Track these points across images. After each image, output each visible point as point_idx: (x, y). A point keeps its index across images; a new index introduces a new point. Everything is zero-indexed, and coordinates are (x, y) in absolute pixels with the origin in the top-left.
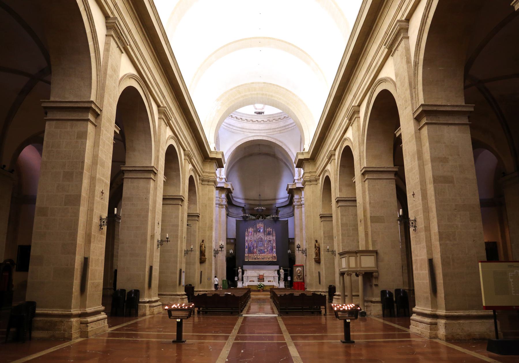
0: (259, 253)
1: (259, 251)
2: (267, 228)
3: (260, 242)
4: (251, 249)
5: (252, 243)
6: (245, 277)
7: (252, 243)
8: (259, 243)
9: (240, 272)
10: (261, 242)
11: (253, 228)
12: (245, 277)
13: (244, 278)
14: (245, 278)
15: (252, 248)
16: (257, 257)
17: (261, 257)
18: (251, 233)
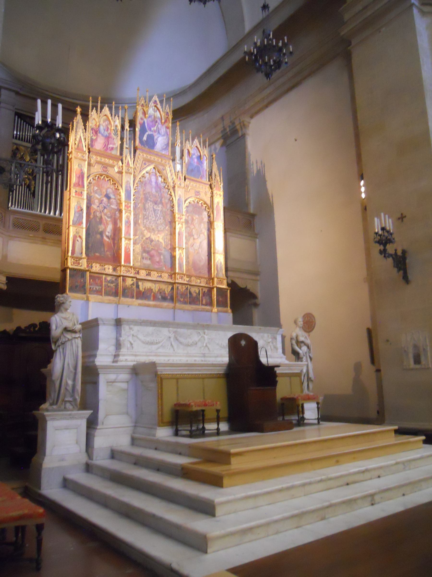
0: (148, 262)
1: (148, 252)
2: (187, 139)
3: (149, 205)
4: (101, 233)
5: (108, 197)
6: (112, 377)
7: (108, 197)
8: (145, 209)
9: (66, 330)
10: (156, 203)
11: (117, 113)
12: (112, 377)
13: (102, 379)
14: (110, 383)
15: (110, 228)
16: (138, 286)
17: (155, 287)
18: (108, 138)
